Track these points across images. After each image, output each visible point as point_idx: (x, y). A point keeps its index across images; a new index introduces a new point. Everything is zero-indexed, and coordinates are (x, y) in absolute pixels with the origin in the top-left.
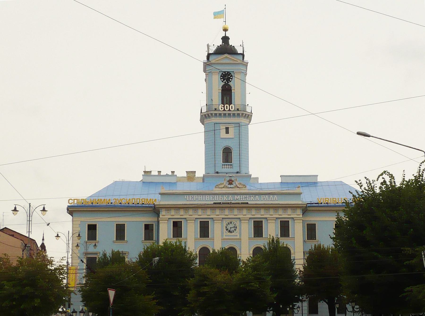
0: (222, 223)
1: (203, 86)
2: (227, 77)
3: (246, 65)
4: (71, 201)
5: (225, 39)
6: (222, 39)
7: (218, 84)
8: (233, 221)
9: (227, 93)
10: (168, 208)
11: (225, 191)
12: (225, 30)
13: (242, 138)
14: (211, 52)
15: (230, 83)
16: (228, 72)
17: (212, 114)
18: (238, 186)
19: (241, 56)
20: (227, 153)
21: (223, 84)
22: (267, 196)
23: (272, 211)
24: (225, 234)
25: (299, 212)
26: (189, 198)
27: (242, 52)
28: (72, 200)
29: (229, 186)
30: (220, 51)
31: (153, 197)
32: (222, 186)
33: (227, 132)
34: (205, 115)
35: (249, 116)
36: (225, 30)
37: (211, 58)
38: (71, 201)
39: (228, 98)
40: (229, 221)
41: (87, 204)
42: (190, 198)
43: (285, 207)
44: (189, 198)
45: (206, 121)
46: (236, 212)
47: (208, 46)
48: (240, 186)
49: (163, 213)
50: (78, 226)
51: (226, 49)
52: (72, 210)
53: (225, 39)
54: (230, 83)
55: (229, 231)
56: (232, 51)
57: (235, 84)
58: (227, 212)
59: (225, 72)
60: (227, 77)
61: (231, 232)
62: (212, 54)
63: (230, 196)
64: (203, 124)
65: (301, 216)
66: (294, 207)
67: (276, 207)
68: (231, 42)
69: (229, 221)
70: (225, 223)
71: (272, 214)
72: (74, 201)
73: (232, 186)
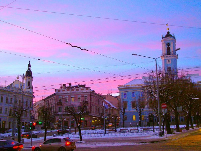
2: (168, 44)
3: (175, 40)
5: (168, 33)
9: (168, 49)
19: (173, 38)
21: (167, 47)
33: (169, 61)
37: (163, 38)
47: (162, 35)
51: (168, 35)
53: (168, 33)
54: (169, 46)
60: (168, 44)
62: (164, 37)
68: (170, 33)
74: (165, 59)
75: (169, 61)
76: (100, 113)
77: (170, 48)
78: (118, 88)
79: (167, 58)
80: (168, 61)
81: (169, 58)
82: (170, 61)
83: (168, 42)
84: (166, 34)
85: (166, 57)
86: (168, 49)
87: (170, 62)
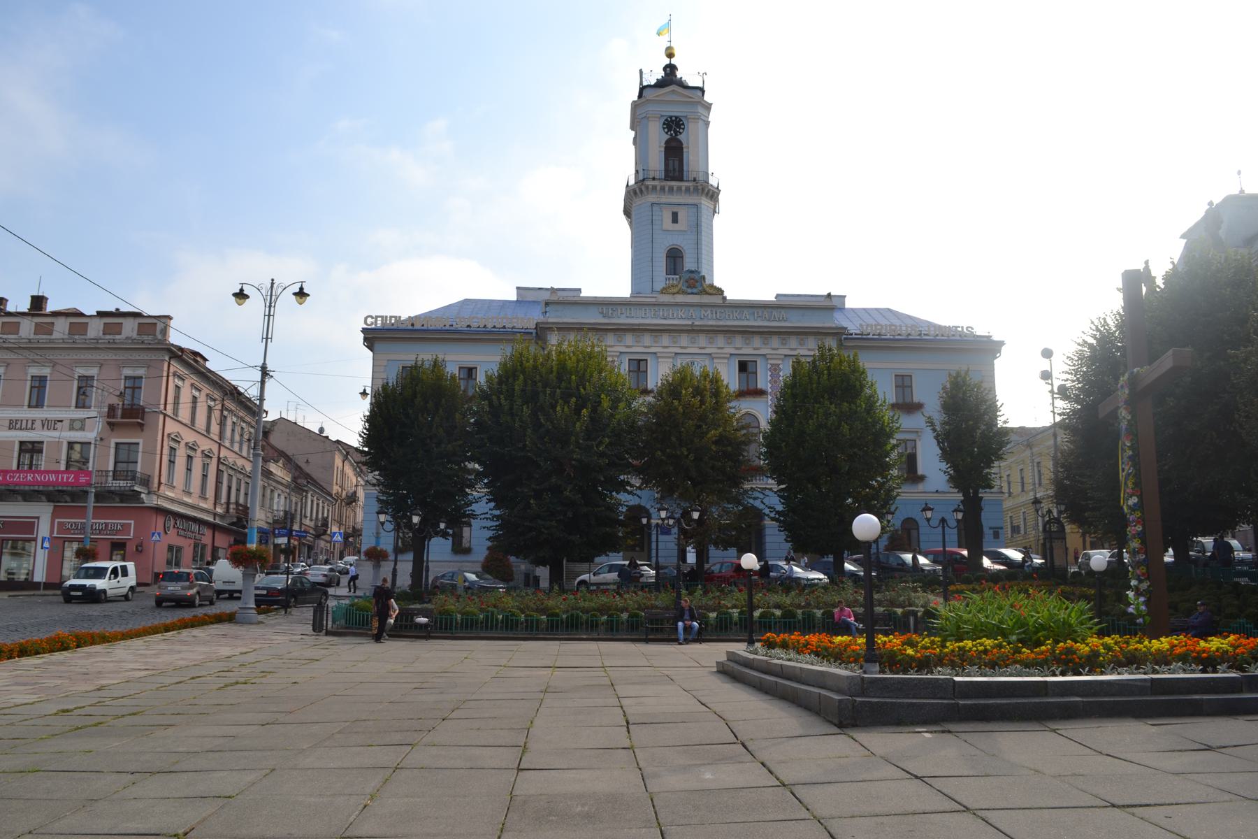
2: (674, 125)
3: (708, 107)
4: (369, 320)
5: (670, 69)
6: (665, 69)
7: (658, 137)
10: (564, 328)
12: (670, 55)
13: (699, 232)
14: (645, 84)
19: (700, 93)
21: (667, 137)
23: (775, 341)
27: (700, 85)
29: (689, 291)
30: (660, 84)
31: (533, 317)
33: (675, 218)
35: (713, 194)
36: (670, 55)
37: (645, 92)
39: (677, 163)
41: (402, 327)
45: (638, 201)
46: (702, 340)
52: (375, 337)
53: (670, 69)
54: (681, 137)
56: (682, 84)
58: (684, 340)
60: (674, 125)
68: (679, 74)
73: (695, 291)
74: (655, 200)
75: (675, 218)
77: (681, 143)
78: (364, 331)
79: (664, 199)
80: (668, 217)
83: (675, 111)
84: (660, 74)
86: (674, 151)
87: (683, 223)
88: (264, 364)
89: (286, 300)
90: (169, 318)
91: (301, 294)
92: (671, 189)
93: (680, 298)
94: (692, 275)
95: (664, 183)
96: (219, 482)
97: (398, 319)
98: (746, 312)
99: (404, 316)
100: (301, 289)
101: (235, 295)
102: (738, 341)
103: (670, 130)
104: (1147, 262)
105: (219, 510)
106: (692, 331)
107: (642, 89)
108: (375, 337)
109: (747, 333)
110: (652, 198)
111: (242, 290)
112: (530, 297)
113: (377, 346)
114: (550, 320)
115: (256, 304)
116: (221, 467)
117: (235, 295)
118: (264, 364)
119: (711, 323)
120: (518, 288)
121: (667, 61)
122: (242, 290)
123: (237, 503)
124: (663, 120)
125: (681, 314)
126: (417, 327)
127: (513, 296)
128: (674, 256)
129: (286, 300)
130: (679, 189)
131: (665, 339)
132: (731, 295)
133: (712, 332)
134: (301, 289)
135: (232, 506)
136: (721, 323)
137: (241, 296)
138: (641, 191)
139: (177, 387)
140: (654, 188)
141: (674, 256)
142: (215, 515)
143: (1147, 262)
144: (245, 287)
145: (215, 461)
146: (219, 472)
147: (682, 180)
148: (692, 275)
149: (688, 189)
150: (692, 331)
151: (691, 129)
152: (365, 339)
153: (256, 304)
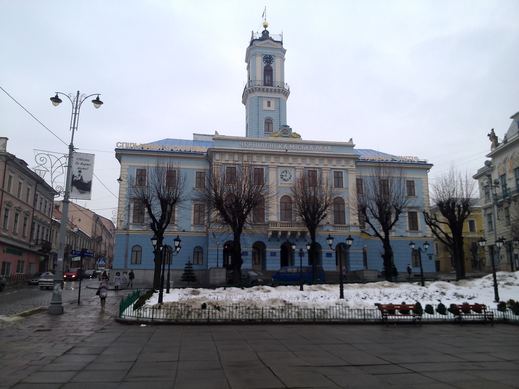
0: (277, 171)
1: (246, 72)
2: (268, 59)
4: (119, 145)
5: (265, 34)
8: (288, 169)
9: (268, 71)
10: (222, 152)
11: (279, 139)
12: (266, 26)
14: (254, 38)
15: (271, 65)
16: (269, 56)
17: (256, 88)
18: (293, 135)
20: (269, 123)
21: (265, 65)
22: (321, 147)
23: (326, 161)
24: (280, 182)
25: (352, 163)
26: (244, 145)
28: (121, 143)
29: (284, 135)
32: (277, 135)
34: (249, 90)
36: (266, 26)
38: (119, 145)
39: (269, 78)
40: (284, 169)
41: (137, 149)
42: (245, 144)
43: (339, 158)
44: (244, 145)
45: (251, 96)
46: (290, 160)
48: (295, 136)
49: (217, 157)
50: (126, 170)
52: (121, 154)
53: (265, 34)
54: (272, 65)
55: (284, 180)
57: (275, 65)
58: (282, 160)
59: (267, 55)
60: (268, 59)
61: (286, 181)
62: (256, 40)
63: (285, 145)
64: (245, 105)
65: (354, 167)
66: (347, 158)
67: (330, 158)
69: (284, 169)
70: (280, 171)
71: (324, 164)
72: (123, 145)
73: (286, 135)
76: (37, 240)
77: (271, 68)
78: (116, 150)
80: (265, 103)
81: (269, 95)
82: (272, 103)
83: (269, 52)
84: (261, 35)
85: (263, 89)
86: (268, 71)
87: (273, 107)
88: (72, 144)
89: (88, 105)
90: (7, 139)
91: (98, 102)
92: (267, 90)
93: (279, 139)
94: (286, 128)
95: (264, 87)
96: (32, 229)
97: (135, 144)
98: (311, 146)
99: (138, 144)
100: (98, 98)
101: (52, 99)
102: (308, 161)
103: (266, 61)
104: (493, 130)
105: (32, 243)
106: (286, 155)
107: (253, 41)
108: (121, 154)
109: (313, 157)
110: (258, 94)
111: (57, 96)
112: (200, 138)
113: (123, 159)
114: (215, 147)
115: (66, 105)
116: (34, 221)
117: (52, 99)
118: (72, 144)
119: (294, 151)
120: (194, 134)
121: (264, 29)
122: (57, 96)
123: (42, 240)
124: (263, 56)
125: (280, 146)
126: (145, 149)
127: (191, 138)
128: (269, 122)
129: (88, 105)
130: (271, 90)
131: (272, 159)
132: (305, 137)
133: (295, 156)
134: (98, 98)
135: (39, 241)
136: (300, 152)
137: (56, 100)
138: (253, 90)
139: (10, 177)
140: (259, 89)
141: (269, 122)
142: (30, 246)
143: (493, 130)
144: (59, 95)
145: (31, 216)
146: (33, 223)
147: (272, 86)
148: (286, 128)
149: (275, 90)
150: (286, 155)
151: (277, 61)
152: (117, 155)
153: (66, 105)
